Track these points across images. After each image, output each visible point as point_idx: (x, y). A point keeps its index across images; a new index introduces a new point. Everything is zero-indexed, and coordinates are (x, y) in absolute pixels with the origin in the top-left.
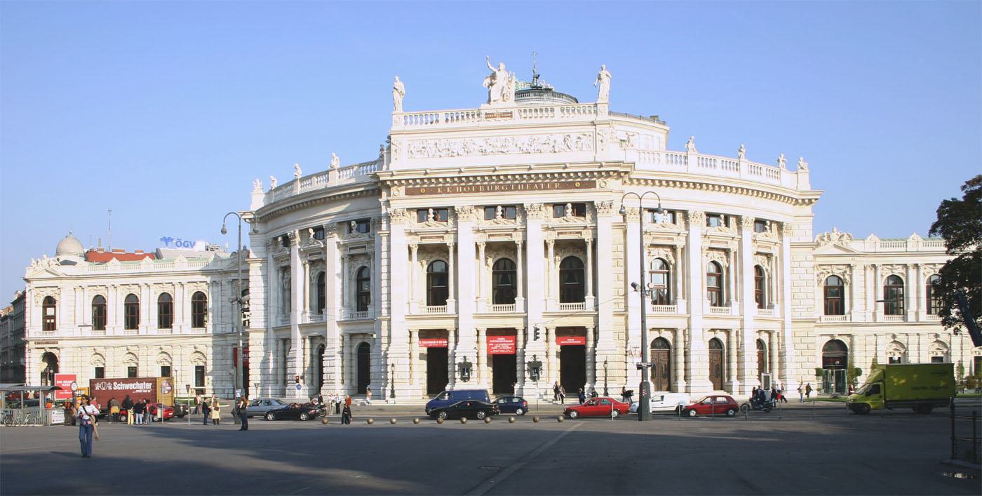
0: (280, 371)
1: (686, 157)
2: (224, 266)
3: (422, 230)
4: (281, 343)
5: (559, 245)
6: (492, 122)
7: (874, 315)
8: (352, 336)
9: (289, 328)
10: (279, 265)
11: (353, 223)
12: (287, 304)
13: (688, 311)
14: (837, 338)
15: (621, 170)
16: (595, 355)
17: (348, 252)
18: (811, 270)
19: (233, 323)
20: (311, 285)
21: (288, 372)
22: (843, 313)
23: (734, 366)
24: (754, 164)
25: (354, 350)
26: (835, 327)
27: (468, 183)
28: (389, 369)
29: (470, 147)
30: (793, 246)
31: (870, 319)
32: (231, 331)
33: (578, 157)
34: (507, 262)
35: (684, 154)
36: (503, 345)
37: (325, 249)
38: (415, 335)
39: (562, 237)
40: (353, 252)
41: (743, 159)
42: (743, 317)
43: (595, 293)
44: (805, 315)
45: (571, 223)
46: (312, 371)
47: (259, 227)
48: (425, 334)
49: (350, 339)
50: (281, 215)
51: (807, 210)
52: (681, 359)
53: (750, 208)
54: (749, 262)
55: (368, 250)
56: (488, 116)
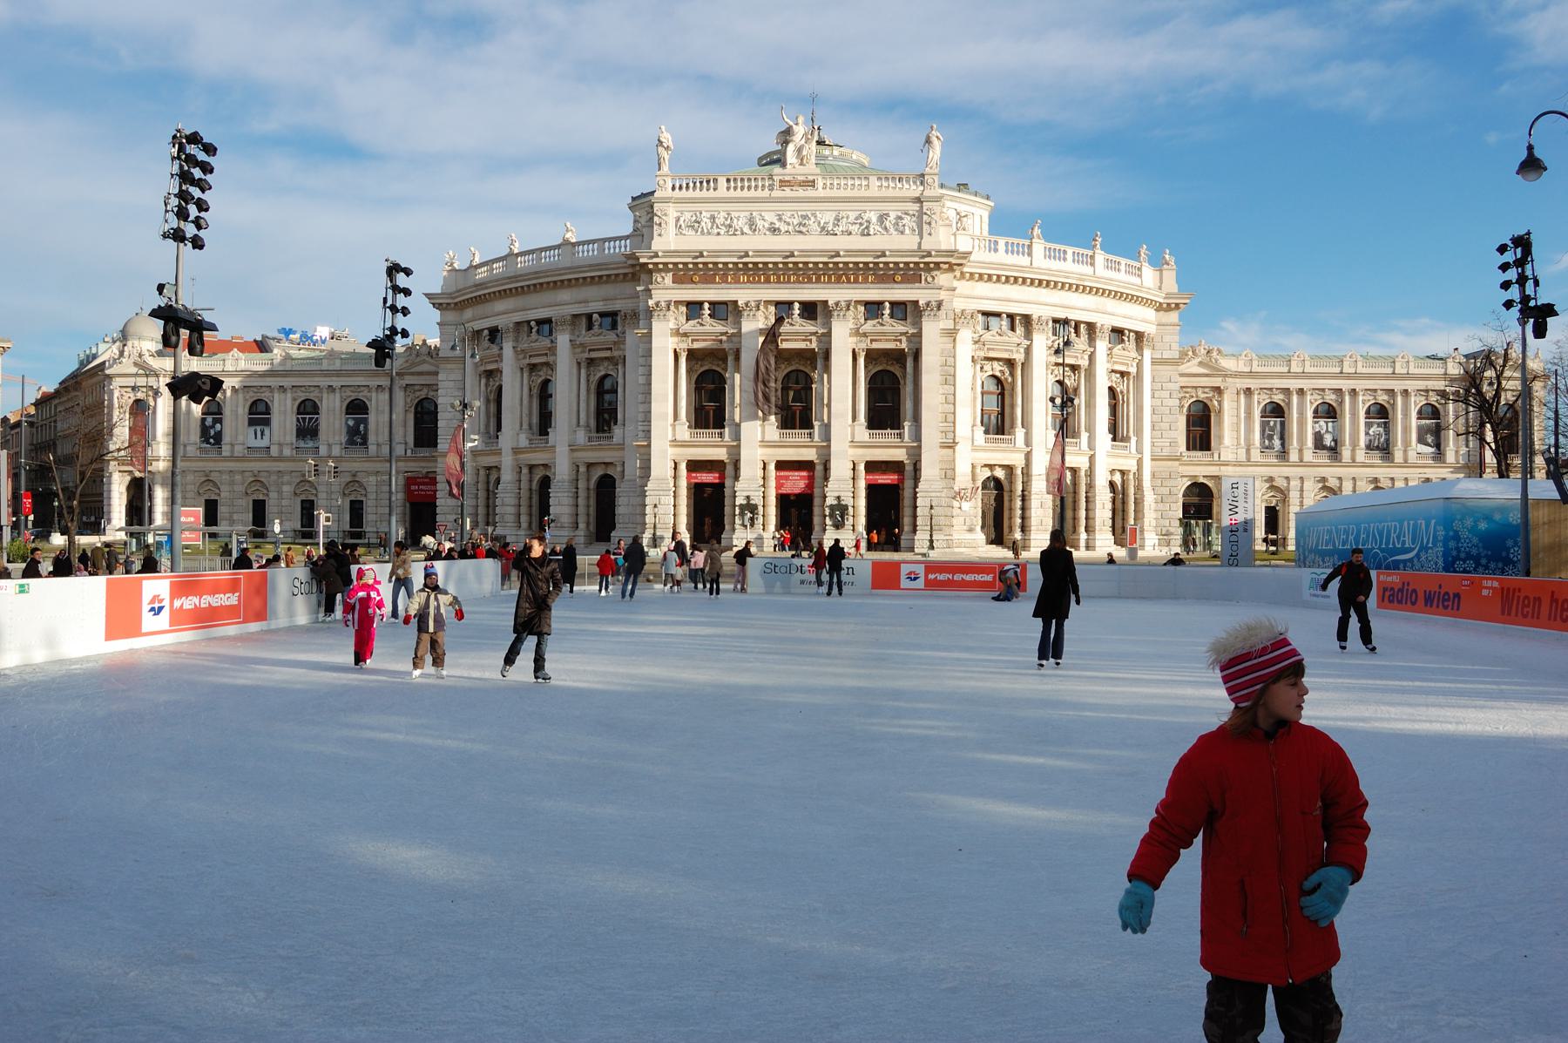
1: (1030, 247)
3: (695, 330)
4: (482, 472)
5: (872, 356)
6: (788, 192)
7: (1248, 451)
8: (589, 466)
9: (499, 453)
11: (595, 316)
13: (1028, 442)
14: (1202, 480)
15: (954, 261)
16: (915, 498)
17: (586, 355)
18: (1177, 395)
20: (531, 396)
22: (1209, 449)
23: (1082, 514)
24: (1111, 257)
25: (592, 485)
26: (1199, 467)
27: (753, 271)
28: (649, 510)
29: (760, 223)
30: (1154, 362)
31: (1242, 456)
33: (898, 243)
34: (801, 376)
35: (1027, 242)
36: (796, 483)
37: (552, 350)
38: (683, 467)
39: (875, 346)
40: (594, 355)
41: (1098, 251)
42: (1098, 456)
43: (917, 419)
44: (1166, 452)
45: (887, 328)
47: (451, 316)
48: (694, 466)
50: (491, 300)
51: (1173, 317)
52: (1019, 503)
53: (1109, 313)
54: (1102, 383)
55: (616, 353)
56: (783, 183)
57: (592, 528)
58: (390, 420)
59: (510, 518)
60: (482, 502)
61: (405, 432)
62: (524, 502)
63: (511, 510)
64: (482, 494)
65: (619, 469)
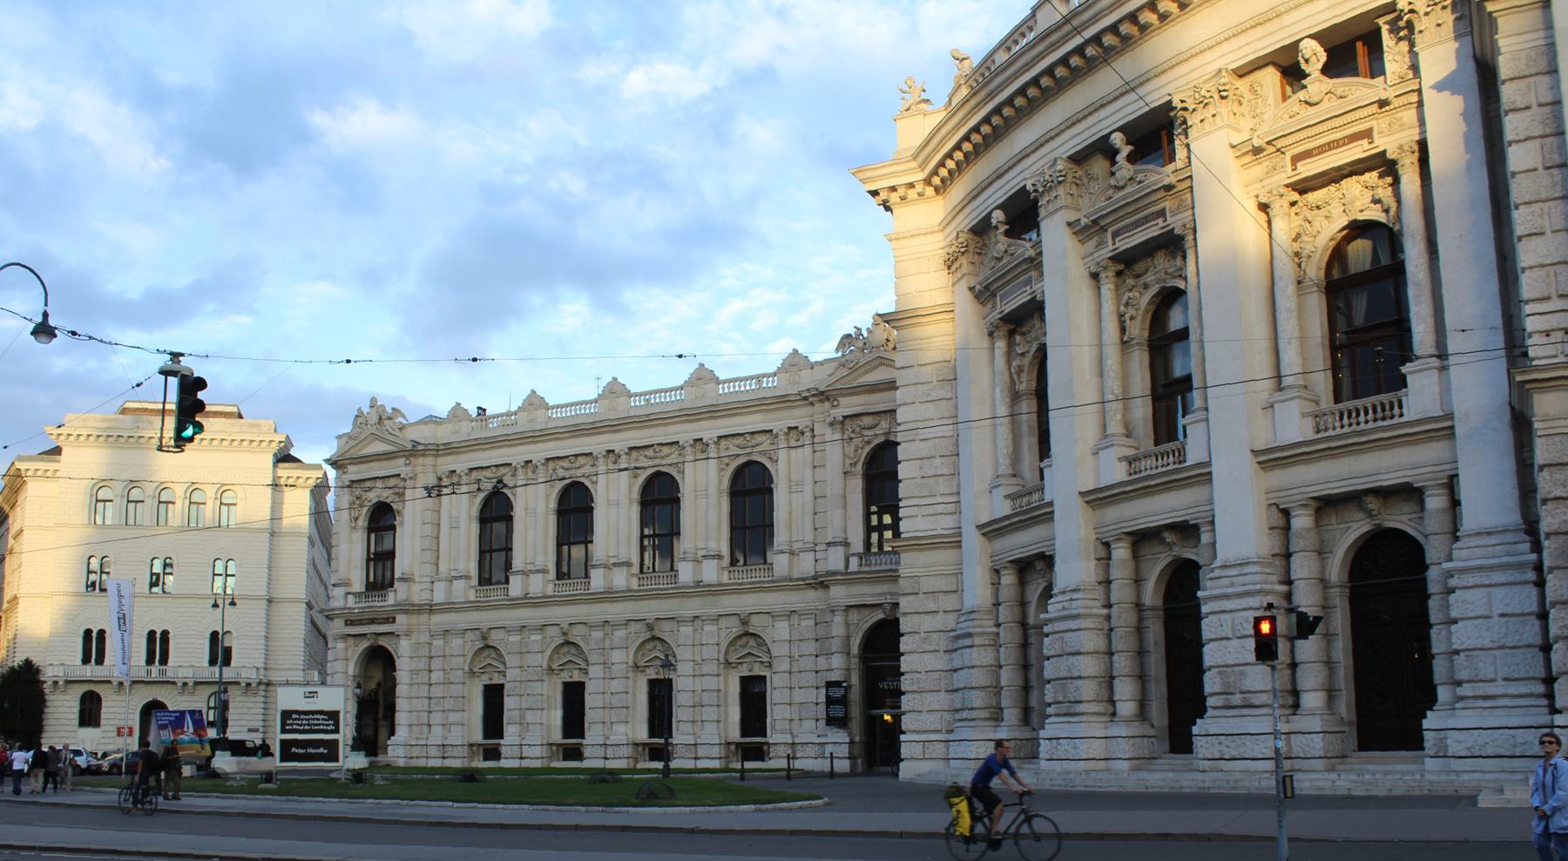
0: (1008, 677)
2: (819, 379)
4: (1009, 578)
8: (1326, 505)
9: (1044, 515)
10: (996, 315)
12: (1030, 444)
19: (846, 544)
21: (1047, 674)
25: (1336, 569)
32: (841, 567)
40: (1308, 169)
46: (1142, 666)
49: (1318, 524)
57: (1345, 706)
58: (814, 498)
59: (1088, 690)
60: (1009, 655)
61: (849, 517)
62: (1123, 641)
63: (1089, 666)
64: (1010, 635)
65: (1435, 502)
